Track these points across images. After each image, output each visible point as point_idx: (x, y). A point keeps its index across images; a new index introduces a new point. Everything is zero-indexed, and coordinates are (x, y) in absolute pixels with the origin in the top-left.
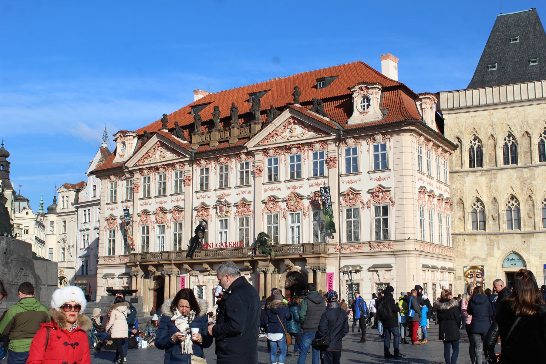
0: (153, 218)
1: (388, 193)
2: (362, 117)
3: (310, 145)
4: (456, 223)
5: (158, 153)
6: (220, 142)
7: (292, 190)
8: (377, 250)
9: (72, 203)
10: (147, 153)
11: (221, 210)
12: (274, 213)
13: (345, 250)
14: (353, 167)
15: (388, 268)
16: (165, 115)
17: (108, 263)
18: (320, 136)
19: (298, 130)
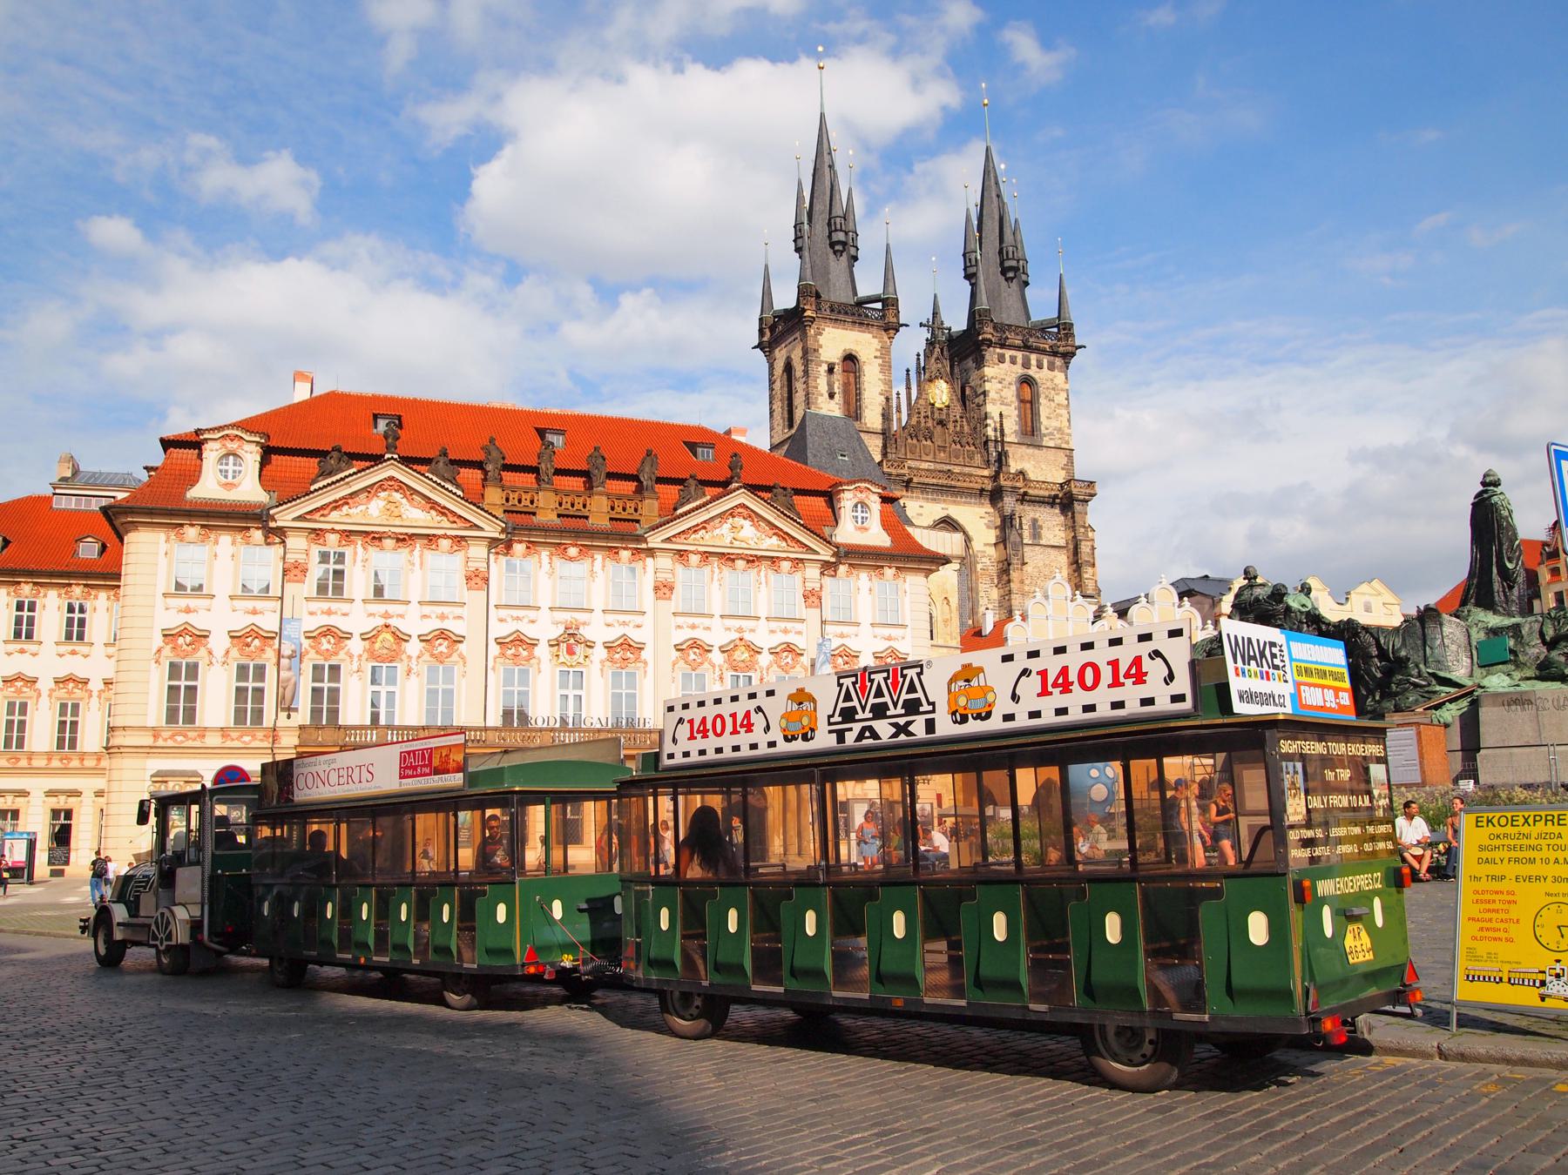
0: (356, 646)
11: (571, 652)
19: (748, 530)
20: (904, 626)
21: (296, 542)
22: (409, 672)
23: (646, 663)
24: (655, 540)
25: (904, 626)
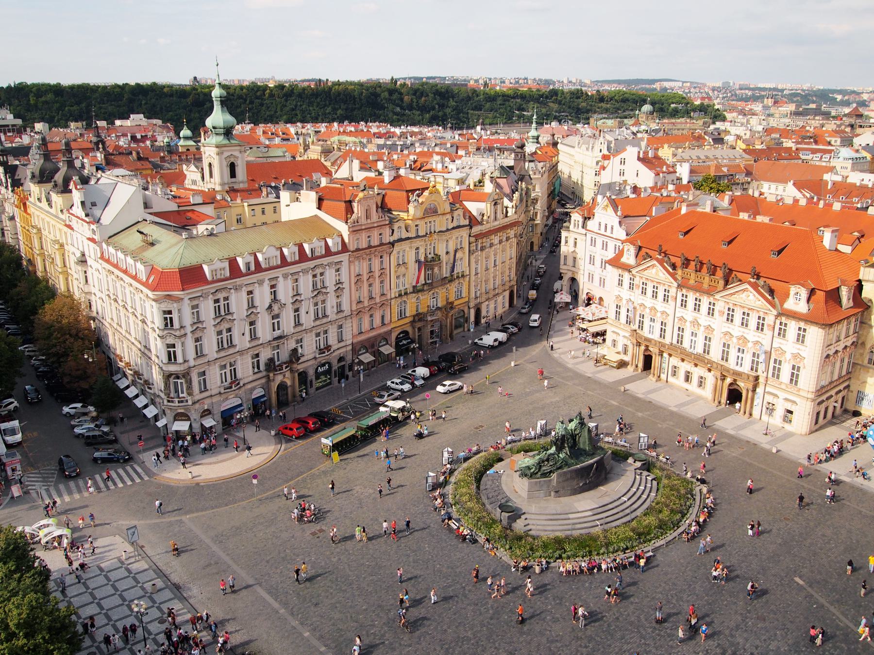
5: (654, 271)
7: (741, 334)
14: (782, 333)
15: (794, 402)
19: (751, 297)
24: (717, 296)
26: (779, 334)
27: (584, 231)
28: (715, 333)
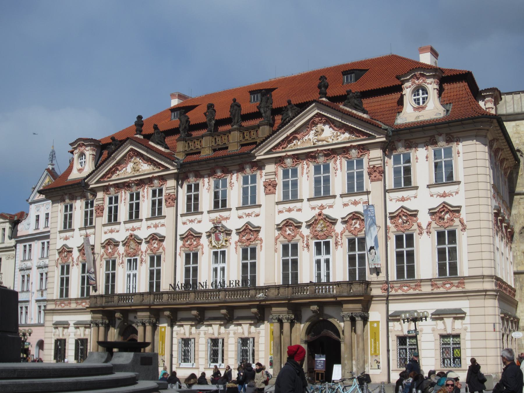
0: (121, 249)
1: (457, 214)
2: (417, 113)
3: (345, 151)
4: (519, 258)
6: (214, 150)
7: (317, 211)
8: (442, 290)
9: (9, 237)
10: (114, 166)
11: (217, 239)
12: (293, 242)
13: (396, 291)
15: (458, 315)
16: (140, 117)
17: (60, 308)
18: (359, 138)
19: (328, 132)
20: (459, 183)
21: (100, 195)
22: (142, 262)
23: (261, 240)
25: (459, 183)
26: (397, 182)
27: (13, 242)
28: (261, 235)
